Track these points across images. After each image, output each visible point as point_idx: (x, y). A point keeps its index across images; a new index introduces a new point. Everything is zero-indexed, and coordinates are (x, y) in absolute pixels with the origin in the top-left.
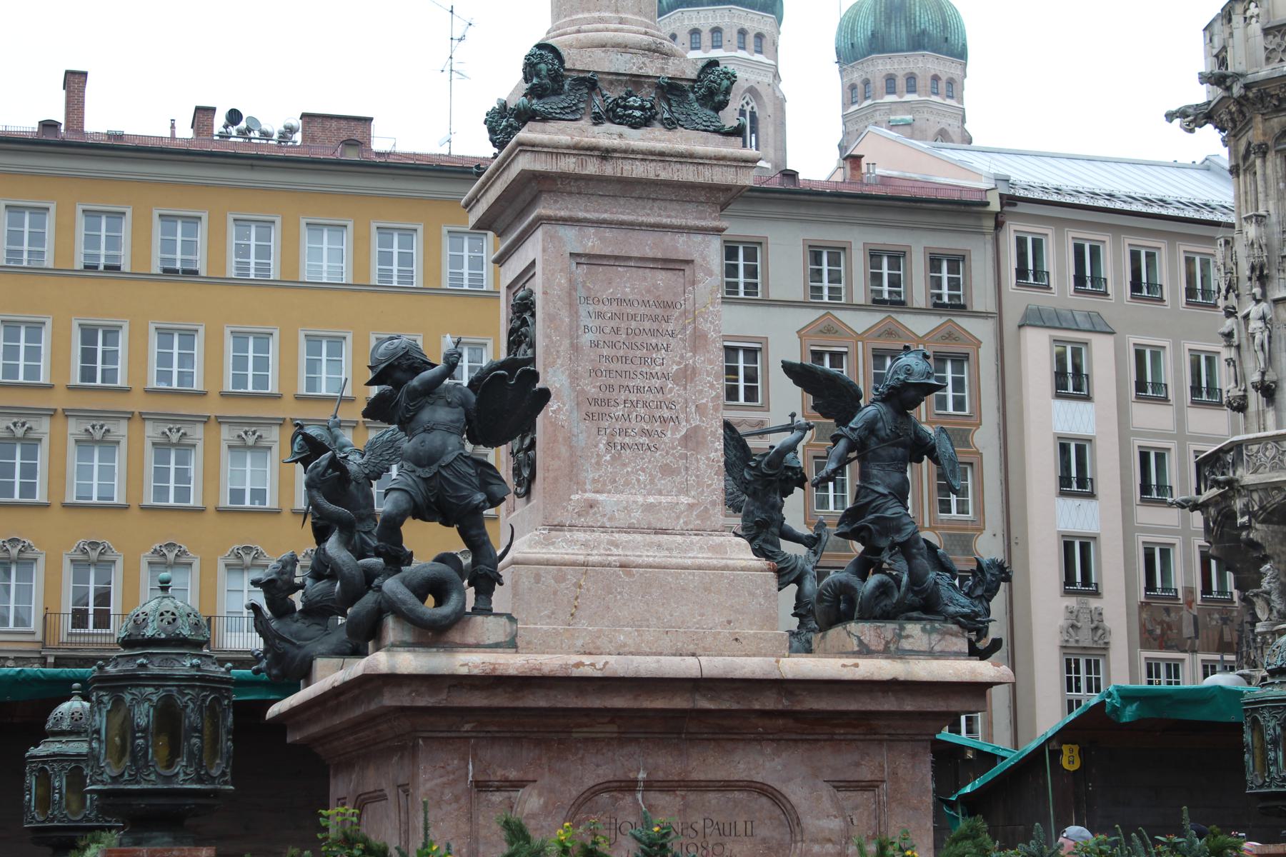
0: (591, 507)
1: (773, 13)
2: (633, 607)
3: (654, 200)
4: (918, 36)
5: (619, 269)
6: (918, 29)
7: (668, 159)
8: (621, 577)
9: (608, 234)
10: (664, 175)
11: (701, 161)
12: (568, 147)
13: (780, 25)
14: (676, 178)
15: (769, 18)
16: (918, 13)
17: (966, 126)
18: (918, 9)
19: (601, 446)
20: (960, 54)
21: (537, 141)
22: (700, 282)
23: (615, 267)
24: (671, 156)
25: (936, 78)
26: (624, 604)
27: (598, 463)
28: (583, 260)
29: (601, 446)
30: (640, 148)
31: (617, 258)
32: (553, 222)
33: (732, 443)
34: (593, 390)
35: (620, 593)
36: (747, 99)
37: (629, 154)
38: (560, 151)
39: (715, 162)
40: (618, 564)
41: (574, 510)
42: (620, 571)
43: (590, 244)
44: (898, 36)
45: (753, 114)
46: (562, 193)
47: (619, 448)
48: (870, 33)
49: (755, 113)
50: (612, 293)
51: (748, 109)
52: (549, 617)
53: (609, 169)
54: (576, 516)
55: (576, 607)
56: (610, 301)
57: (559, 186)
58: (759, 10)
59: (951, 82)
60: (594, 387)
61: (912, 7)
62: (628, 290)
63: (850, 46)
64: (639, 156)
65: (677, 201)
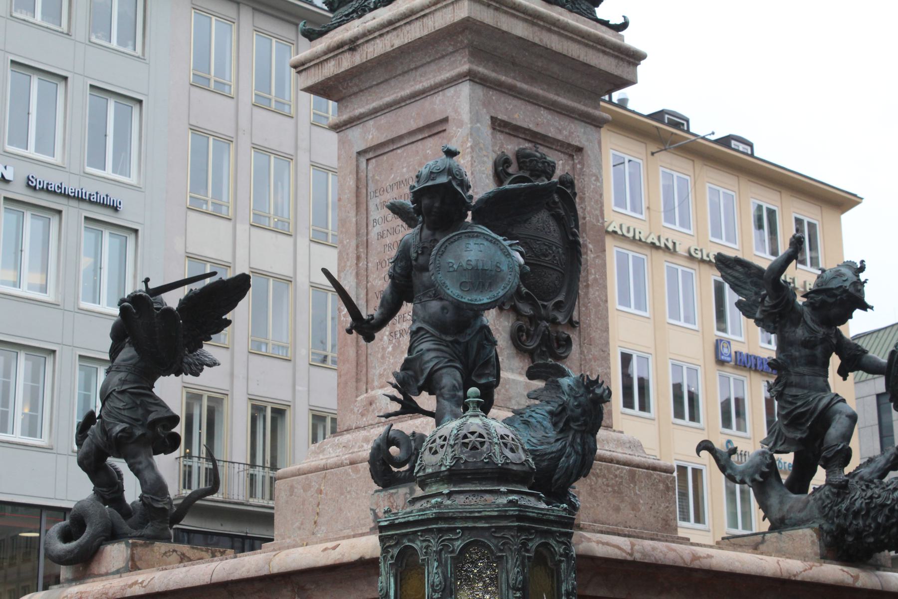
0: (371, 404)
2: (359, 505)
3: (416, 68)
5: (399, 151)
7: (397, 25)
8: (350, 476)
9: (383, 120)
10: (398, 43)
11: (422, 13)
12: (325, 53)
14: (406, 42)
19: (385, 338)
21: (303, 59)
22: (453, 137)
23: (395, 151)
24: (399, 20)
26: (352, 503)
27: (383, 357)
28: (371, 155)
29: (385, 338)
30: (373, 26)
31: (393, 141)
32: (344, 128)
33: (749, 281)
34: (379, 282)
35: (349, 492)
37: (368, 36)
38: (321, 59)
39: (433, 8)
40: (348, 462)
41: (358, 411)
42: (348, 469)
43: (370, 137)
46: (350, 96)
47: (398, 335)
50: (393, 178)
52: (299, 528)
53: (358, 58)
54: (360, 416)
55: (318, 513)
56: (391, 187)
57: (344, 91)
60: (380, 280)
62: (405, 170)
64: (377, 34)
65: (432, 61)
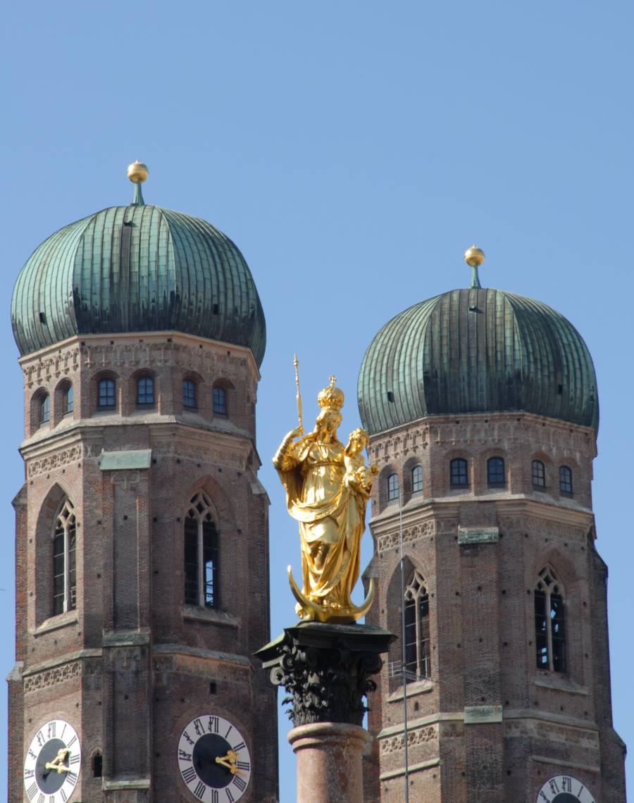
1: (247, 345)
4: (510, 382)
6: (509, 369)
13: (258, 369)
15: (240, 352)
16: (508, 342)
17: (598, 544)
18: (508, 333)
20: (588, 417)
25: (540, 460)
36: (200, 499)
44: (473, 381)
45: (210, 527)
48: (421, 376)
49: (213, 525)
51: (201, 518)
58: (222, 340)
59: (566, 469)
61: (499, 329)
63: (385, 397)
